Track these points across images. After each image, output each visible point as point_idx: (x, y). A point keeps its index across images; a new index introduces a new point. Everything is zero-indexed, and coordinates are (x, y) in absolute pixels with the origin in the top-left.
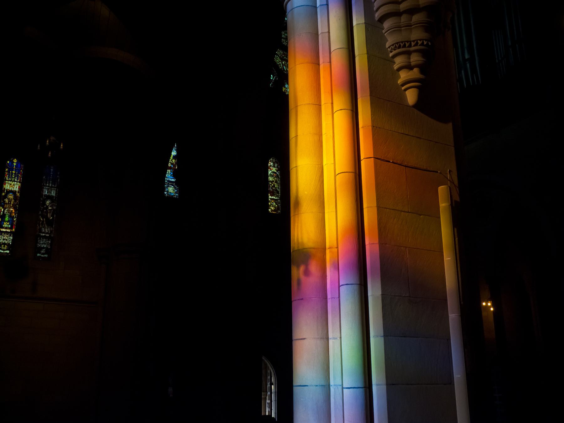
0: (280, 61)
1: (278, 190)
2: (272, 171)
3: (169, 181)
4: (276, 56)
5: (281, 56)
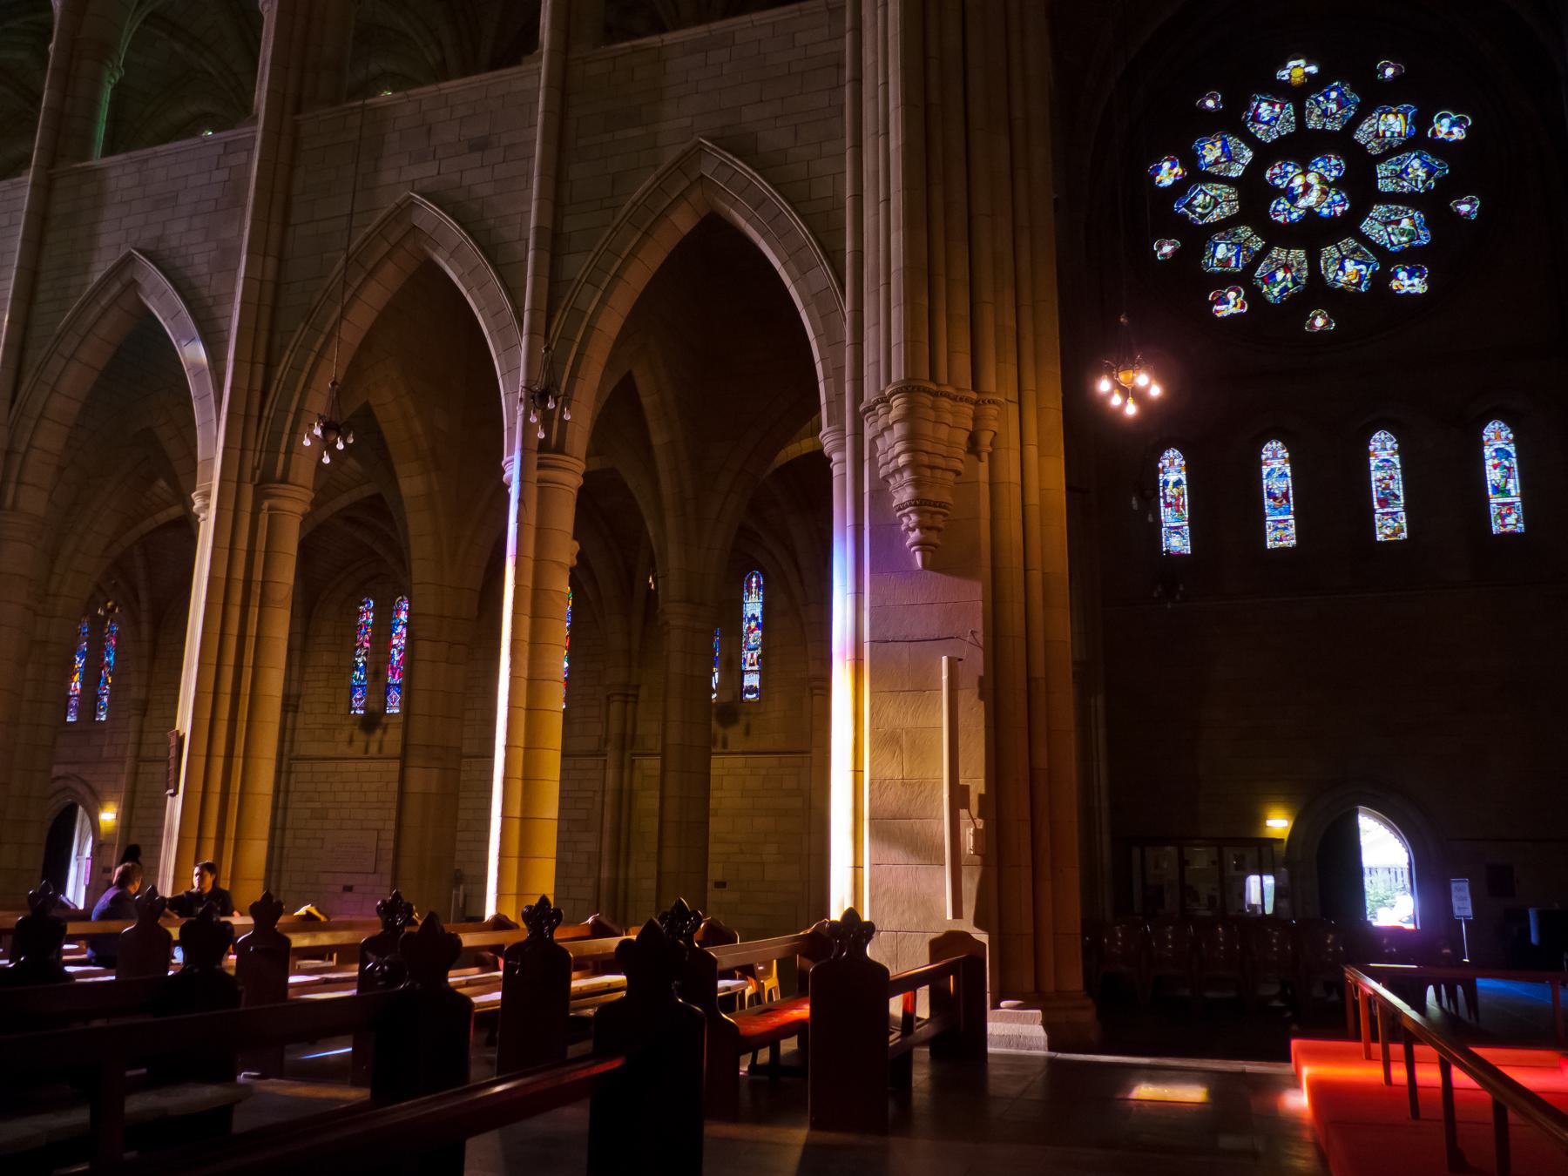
0: (1383, 228)
1: (1397, 492)
2: (1382, 458)
3: (1170, 528)
5: (1383, 217)
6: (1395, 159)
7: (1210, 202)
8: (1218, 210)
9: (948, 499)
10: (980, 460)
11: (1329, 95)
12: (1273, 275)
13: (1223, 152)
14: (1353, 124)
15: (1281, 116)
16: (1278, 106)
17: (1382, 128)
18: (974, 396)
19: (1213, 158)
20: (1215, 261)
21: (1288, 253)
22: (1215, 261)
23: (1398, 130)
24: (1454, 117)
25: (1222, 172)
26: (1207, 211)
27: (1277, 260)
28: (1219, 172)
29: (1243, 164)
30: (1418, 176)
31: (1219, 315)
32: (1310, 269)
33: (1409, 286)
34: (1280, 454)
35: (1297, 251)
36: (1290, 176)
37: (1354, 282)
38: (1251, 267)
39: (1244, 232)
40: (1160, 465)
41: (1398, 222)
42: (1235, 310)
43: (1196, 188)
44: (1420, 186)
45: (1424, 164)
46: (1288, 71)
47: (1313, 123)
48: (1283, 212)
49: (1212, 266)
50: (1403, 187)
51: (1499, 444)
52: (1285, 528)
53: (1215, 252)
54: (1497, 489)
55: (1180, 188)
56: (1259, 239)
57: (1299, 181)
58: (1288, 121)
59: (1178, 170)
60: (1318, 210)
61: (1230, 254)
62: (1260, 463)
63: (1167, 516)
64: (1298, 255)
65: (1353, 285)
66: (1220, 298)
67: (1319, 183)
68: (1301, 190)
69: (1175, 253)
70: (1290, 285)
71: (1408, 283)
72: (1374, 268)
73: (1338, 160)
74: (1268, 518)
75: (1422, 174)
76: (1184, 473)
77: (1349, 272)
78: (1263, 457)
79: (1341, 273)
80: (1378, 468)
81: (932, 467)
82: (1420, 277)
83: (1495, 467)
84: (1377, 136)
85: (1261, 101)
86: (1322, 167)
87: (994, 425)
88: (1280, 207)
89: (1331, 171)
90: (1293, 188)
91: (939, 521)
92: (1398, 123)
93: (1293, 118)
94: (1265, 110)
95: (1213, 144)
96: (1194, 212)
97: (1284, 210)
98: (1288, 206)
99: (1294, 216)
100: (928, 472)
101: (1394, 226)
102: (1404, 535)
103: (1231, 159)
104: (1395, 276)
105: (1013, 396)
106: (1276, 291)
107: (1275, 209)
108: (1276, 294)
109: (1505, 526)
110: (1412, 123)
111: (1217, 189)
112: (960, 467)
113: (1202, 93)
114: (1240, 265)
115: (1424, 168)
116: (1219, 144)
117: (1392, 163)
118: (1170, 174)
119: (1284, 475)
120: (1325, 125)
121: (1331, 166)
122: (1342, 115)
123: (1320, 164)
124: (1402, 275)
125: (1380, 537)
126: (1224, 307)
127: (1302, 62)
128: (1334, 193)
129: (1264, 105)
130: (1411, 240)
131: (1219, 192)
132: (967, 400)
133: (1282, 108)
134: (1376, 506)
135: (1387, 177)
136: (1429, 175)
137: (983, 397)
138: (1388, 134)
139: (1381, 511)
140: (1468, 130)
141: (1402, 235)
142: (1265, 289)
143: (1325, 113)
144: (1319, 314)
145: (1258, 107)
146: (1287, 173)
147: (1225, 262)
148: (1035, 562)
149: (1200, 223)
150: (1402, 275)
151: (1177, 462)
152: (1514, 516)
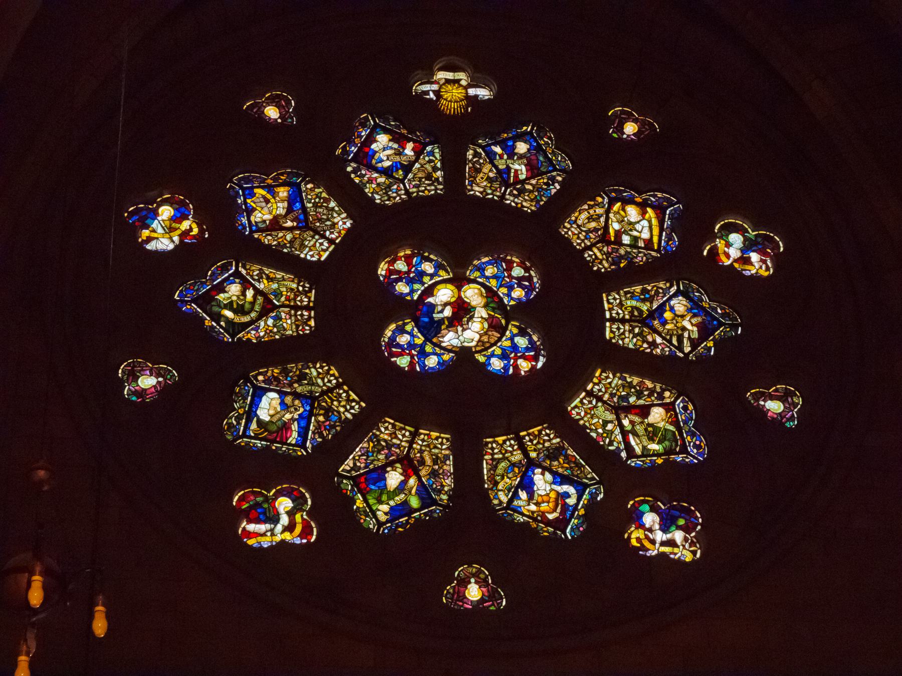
0: (610, 416)
4: (590, 402)
5: (612, 395)
6: (638, 289)
7: (253, 303)
8: (270, 322)
11: (514, 147)
12: (379, 474)
13: (290, 210)
15: (417, 165)
16: (410, 146)
19: (268, 217)
20: (254, 426)
21: (414, 435)
22: (254, 426)
23: (645, 235)
24: (752, 234)
25: (285, 246)
27: (389, 446)
29: (331, 241)
30: (684, 329)
32: (457, 475)
33: (663, 544)
35: (434, 434)
37: (551, 517)
41: (644, 411)
43: (225, 268)
44: (687, 349)
45: (695, 307)
46: (435, 87)
49: (244, 435)
50: (653, 344)
53: (255, 404)
56: (353, 396)
58: (429, 177)
60: (481, 359)
65: (548, 523)
66: (258, 505)
67: (486, 306)
68: (448, 312)
69: (163, 391)
70: (415, 502)
72: (593, 496)
73: (527, 270)
75: (690, 325)
79: (523, 495)
82: (686, 529)
84: (604, 238)
86: (495, 277)
88: (404, 339)
89: (511, 288)
90: (432, 307)
92: (645, 223)
95: (270, 189)
96: (217, 317)
97: (411, 346)
101: (637, 419)
103: (305, 225)
104: (636, 518)
107: (392, 341)
108: (383, 518)
110: (672, 229)
111: (269, 279)
114: (308, 444)
115: (695, 315)
116: (283, 192)
118: (171, 230)
123: (490, 271)
124: (650, 519)
126: (262, 528)
127: (462, 76)
128: (515, 331)
129: (383, 139)
130: (668, 452)
131: (275, 286)
133: (418, 152)
135: (623, 321)
136: (705, 331)
138: (626, 239)
140: (778, 260)
141: (651, 440)
142: (359, 503)
143: (503, 177)
144: (474, 575)
145: (371, 139)
146: (422, 274)
149: (228, 338)
150: (650, 519)
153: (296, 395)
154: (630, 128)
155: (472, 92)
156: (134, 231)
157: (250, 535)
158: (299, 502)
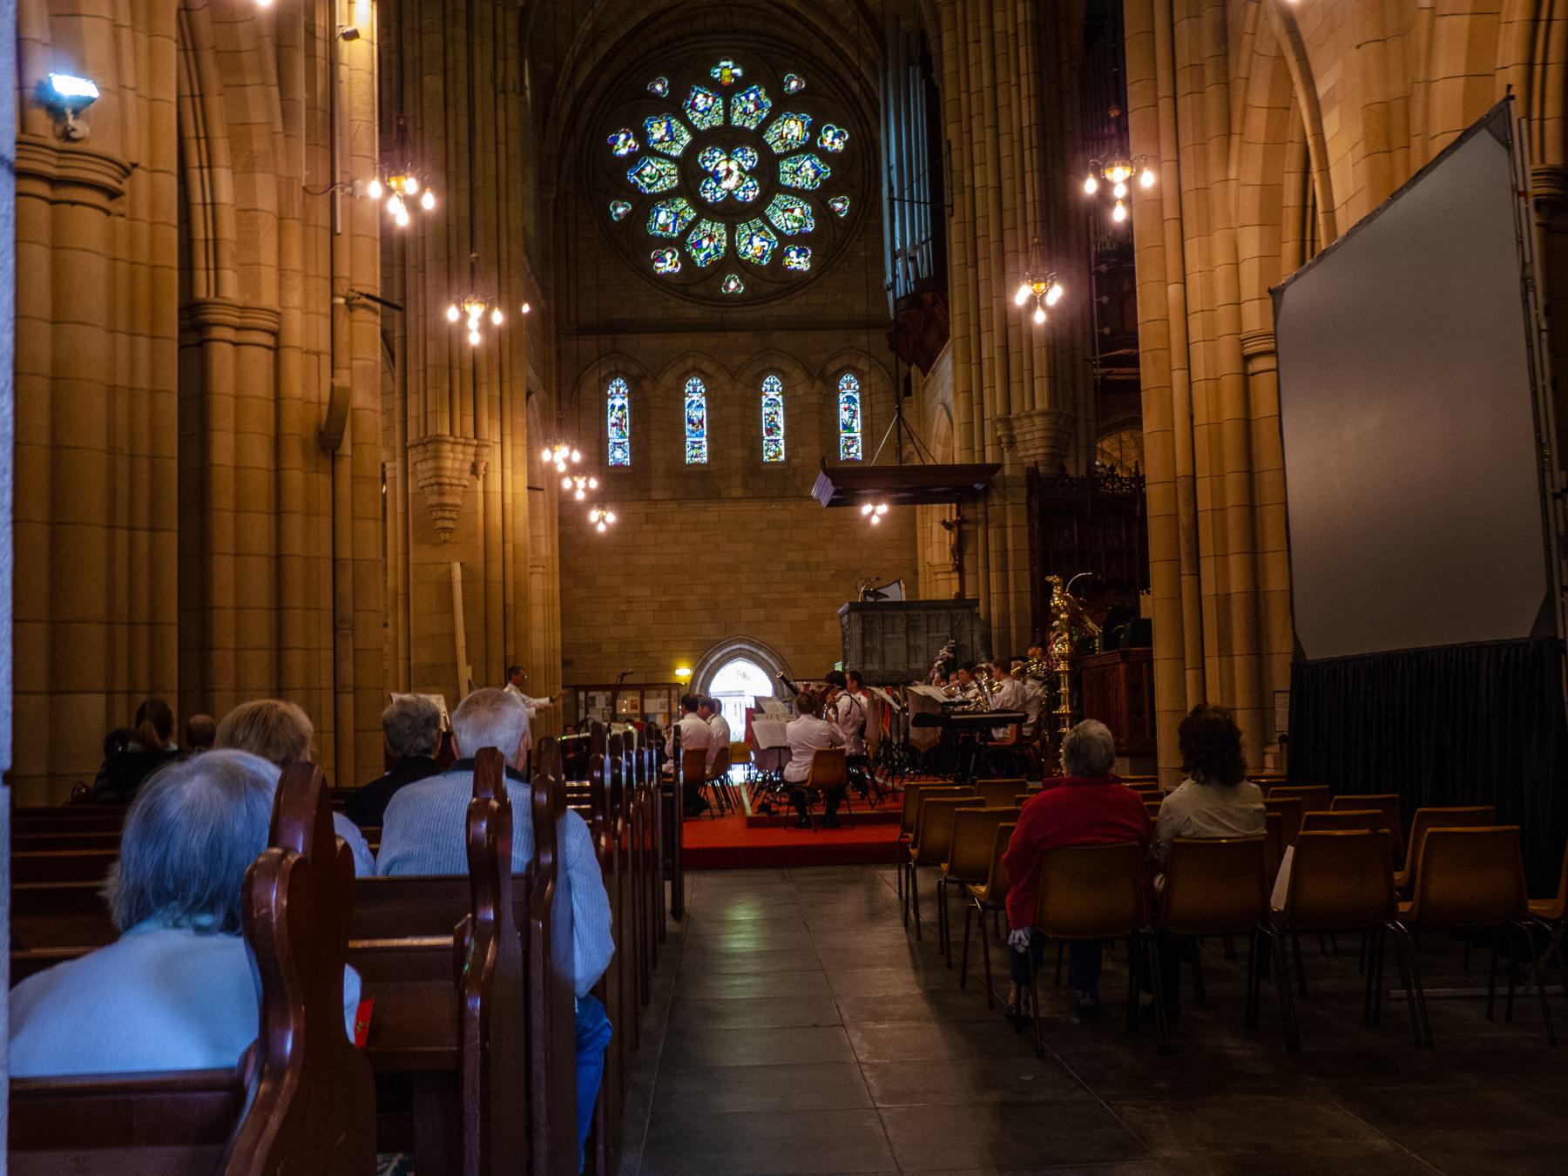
3: (615, 443)
9: (458, 501)
10: (478, 478)
12: (700, 242)
13: (667, 133)
14: (764, 126)
17: (786, 131)
18: (475, 442)
21: (713, 225)
24: (836, 130)
26: (653, 181)
28: (664, 149)
31: (658, 271)
34: (698, 388)
36: (717, 161)
38: (684, 234)
39: (682, 204)
40: (609, 392)
41: (792, 211)
42: (670, 269)
43: (645, 160)
45: (813, 166)
47: (737, 120)
48: (712, 193)
50: (797, 182)
51: (849, 393)
52: (700, 448)
54: (846, 427)
55: (633, 159)
57: (723, 167)
59: (631, 142)
60: (736, 192)
61: (669, 221)
62: (685, 395)
63: (612, 433)
64: (719, 230)
68: (724, 174)
70: (713, 252)
71: (798, 261)
74: (688, 439)
75: (811, 173)
76: (627, 399)
77: (755, 247)
78: (686, 391)
79: (750, 247)
80: (767, 404)
81: (451, 485)
82: (806, 257)
83: (845, 410)
84: (781, 137)
85: (698, 92)
87: (486, 459)
88: (708, 186)
90: (718, 172)
91: (454, 515)
93: (721, 112)
94: (700, 101)
95: (659, 123)
96: (643, 181)
97: (711, 188)
98: (714, 185)
99: (718, 195)
100: (448, 488)
102: (782, 457)
103: (672, 139)
105: (497, 439)
106: (702, 256)
109: (849, 454)
110: (807, 130)
112: (467, 483)
113: (653, 78)
116: (664, 125)
117: (790, 161)
119: (700, 406)
120: (744, 121)
121: (748, 158)
122: (758, 115)
123: (740, 154)
124: (793, 254)
125: (766, 458)
127: (730, 64)
129: (700, 97)
130: (800, 227)
132: (472, 445)
133: (714, 101)
134: (765, 435)
136: (817, 174)
137: (481, 442)
138: (789, 137)
139: (767, 438)
142: (694, 253)
143: (745, 109)
145: (695, 97)
146: (714, 158)
147: (665, 227)
148: (509, 537)
149: (647, 191)
150: (793, 254)
151: (622, 390)
152: (855, 447)
153: (671, 212)
154: (794, 84)
155: (734, 71)
156: (612, 146)
157: (657, 268)
158: (674, 253)
